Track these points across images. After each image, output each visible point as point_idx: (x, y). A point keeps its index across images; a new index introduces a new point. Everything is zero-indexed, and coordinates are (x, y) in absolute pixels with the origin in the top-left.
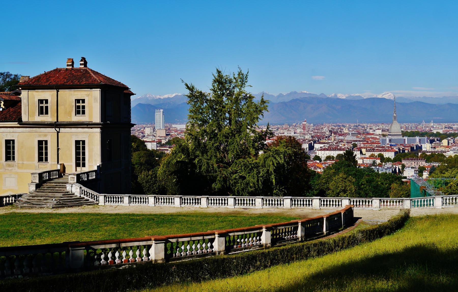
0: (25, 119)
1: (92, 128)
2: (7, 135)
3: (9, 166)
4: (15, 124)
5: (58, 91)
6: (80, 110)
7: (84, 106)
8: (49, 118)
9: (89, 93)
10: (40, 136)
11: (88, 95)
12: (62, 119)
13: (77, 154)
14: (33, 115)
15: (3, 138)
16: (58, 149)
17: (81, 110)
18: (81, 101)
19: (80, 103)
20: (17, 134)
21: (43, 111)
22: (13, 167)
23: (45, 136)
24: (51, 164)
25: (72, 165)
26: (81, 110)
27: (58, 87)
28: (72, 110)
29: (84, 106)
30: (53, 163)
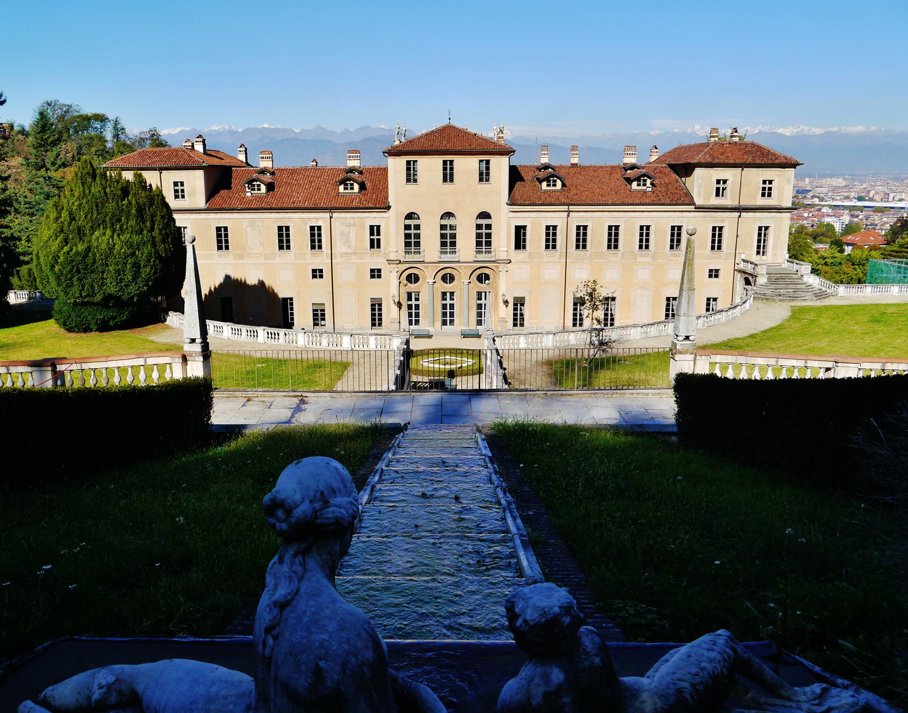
0: (698, 201)
1: (780, 212)
2: (674, 220)
3: (674, 255)
4: (692, 208)
5: (743, 169)
6: (767, 192)
7: (771, 188)
8: (728, 200)
9: (780, 173)
10: (715, 221)
11: (779, 176)
12: (745, 202)
13: (759, 241)
15: (668, 224)
16: (737, 237)
18: (767, 182)
19: (766, 184)
20: (687, 219)
22: (679, 256)
23: (722, 221)
27: (743, 166)
29: (771, 188)
30: (729, 252)
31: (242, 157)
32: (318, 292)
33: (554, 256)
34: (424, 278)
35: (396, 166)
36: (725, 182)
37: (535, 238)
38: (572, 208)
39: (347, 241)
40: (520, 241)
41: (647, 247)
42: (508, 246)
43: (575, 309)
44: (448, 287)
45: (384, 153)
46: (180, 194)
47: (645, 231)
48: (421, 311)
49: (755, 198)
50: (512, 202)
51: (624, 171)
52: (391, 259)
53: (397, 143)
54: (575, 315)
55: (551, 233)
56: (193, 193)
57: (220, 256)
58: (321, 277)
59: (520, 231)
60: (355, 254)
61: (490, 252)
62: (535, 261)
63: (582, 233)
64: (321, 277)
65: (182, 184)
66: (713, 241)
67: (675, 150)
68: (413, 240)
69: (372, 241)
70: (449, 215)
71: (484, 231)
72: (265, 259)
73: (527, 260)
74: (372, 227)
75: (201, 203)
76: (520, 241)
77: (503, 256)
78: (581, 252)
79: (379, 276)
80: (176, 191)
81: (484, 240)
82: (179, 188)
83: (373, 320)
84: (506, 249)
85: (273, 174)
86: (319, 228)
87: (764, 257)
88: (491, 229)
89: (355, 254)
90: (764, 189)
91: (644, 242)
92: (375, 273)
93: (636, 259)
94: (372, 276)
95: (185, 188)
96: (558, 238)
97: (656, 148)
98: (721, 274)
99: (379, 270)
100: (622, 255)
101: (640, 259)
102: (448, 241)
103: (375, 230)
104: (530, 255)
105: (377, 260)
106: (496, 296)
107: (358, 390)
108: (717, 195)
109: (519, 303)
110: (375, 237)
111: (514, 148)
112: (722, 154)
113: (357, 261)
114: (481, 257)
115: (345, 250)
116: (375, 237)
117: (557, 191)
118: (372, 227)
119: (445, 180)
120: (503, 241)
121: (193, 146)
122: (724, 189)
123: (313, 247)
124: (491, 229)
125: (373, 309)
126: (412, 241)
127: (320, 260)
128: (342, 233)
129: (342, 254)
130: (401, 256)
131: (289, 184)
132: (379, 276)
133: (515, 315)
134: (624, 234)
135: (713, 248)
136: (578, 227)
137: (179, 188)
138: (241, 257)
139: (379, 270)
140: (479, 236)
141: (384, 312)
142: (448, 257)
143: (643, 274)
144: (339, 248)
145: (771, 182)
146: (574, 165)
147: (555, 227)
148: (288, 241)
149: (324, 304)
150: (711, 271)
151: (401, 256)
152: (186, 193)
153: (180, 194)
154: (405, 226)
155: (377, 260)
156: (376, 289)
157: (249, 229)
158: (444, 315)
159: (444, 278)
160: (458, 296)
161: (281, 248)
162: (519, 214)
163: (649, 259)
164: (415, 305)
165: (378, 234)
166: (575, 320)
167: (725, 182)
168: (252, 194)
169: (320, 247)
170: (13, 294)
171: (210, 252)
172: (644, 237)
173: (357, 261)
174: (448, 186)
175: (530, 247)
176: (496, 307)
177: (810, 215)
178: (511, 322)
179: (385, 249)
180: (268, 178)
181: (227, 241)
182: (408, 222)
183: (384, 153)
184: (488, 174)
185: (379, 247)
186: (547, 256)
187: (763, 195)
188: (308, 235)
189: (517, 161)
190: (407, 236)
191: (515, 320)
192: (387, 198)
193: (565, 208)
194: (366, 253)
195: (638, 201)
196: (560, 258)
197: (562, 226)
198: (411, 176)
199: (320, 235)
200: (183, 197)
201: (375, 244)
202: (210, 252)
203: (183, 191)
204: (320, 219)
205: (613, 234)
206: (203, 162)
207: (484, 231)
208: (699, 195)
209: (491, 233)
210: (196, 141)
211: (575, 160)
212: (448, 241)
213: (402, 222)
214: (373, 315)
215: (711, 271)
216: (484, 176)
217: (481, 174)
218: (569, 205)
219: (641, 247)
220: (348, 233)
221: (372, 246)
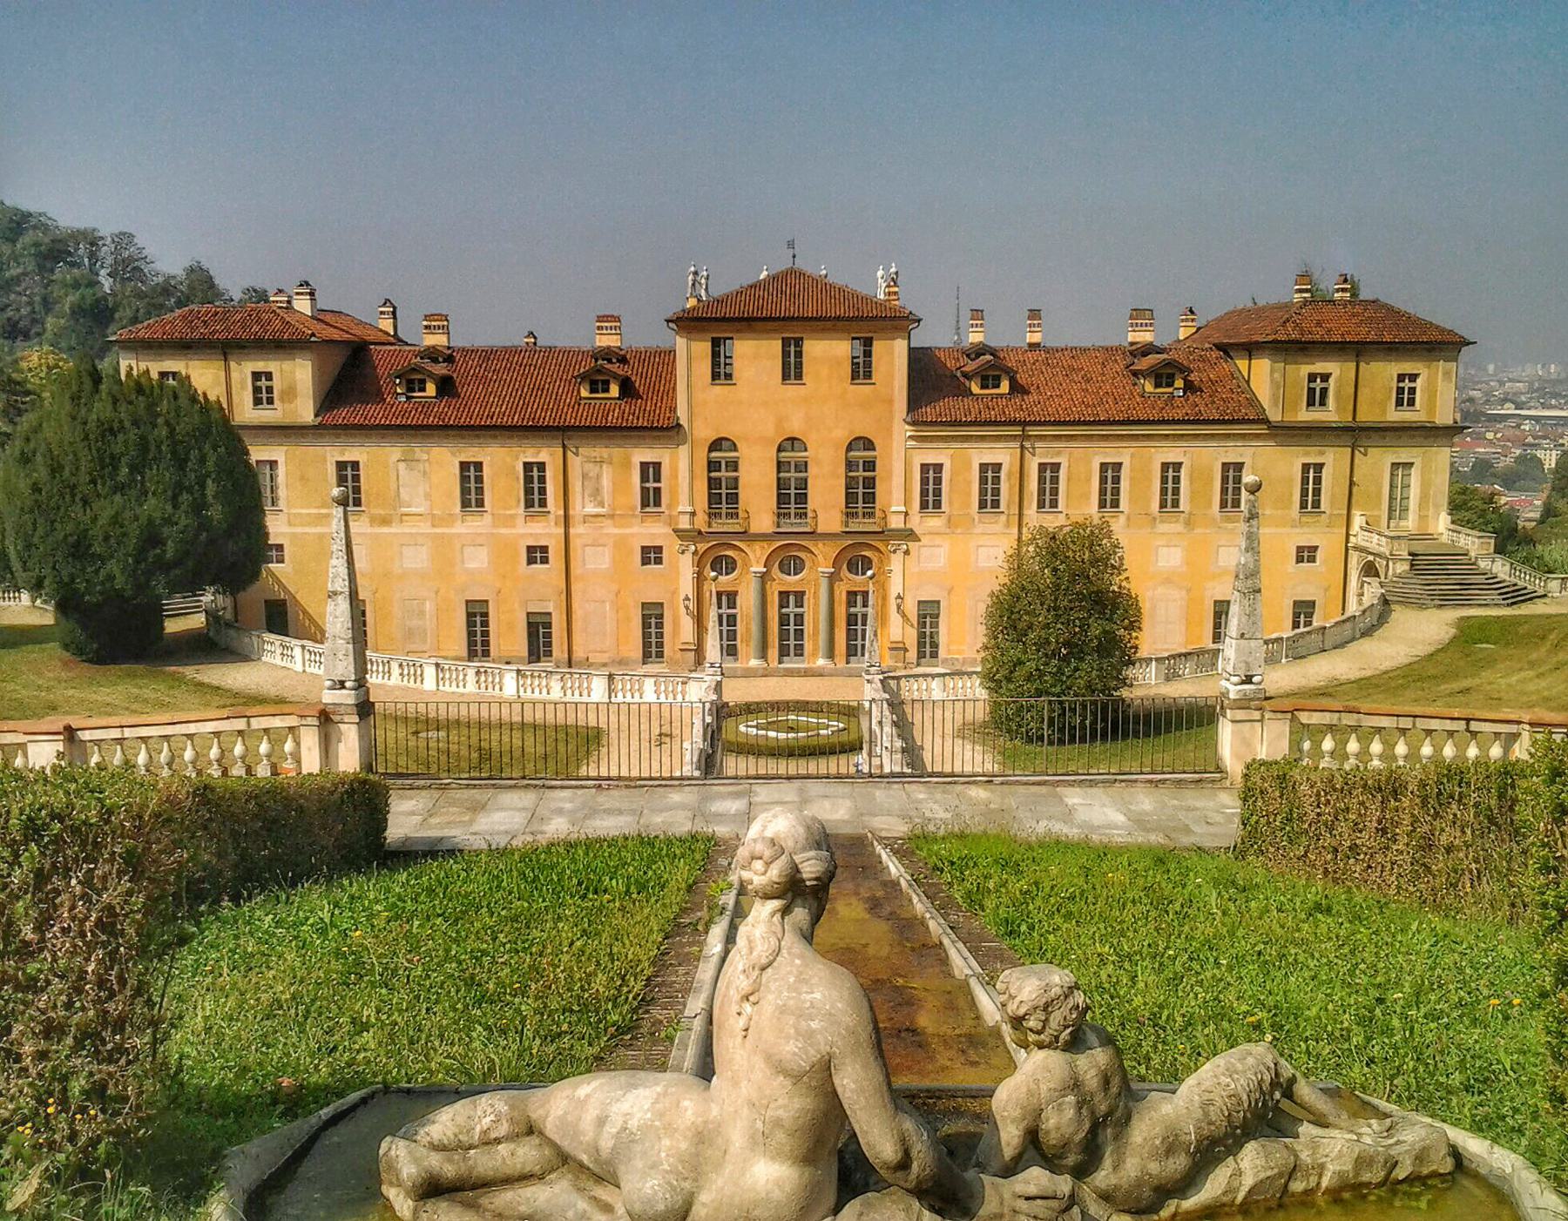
3: (1229, 520)
6: (1405, 398)
8: (1330, 414)
14: (1295, 409)
16: (1352, 483)
17: (1406, 396)
21: (1316, 398)
24: (1331, 515)
25: (1379, 517)
26: (1406, 396)
28: (1390, 397)
31: (386, 325)
33: (996, 522)
34: (747, 565)
35: (692, 354)
36: (1325, 377)
37: (961, 487)
39: (597, 492)
40: (931, 498)
45: (668, 321)
46: (264, 395)
48: (740, 628)
49: (1383, 405)
51: (1129, 359)
52: (681, 526)
53: (692, 302)
56: (290, 393)
58: (545, 560)
59: (931, 475)
60: (612, 516)
61: (872, 515)
62: (959, 531)
64: (545, 560)
65: (269, 376)
66: (1304, 493)
67: (1229, 314)
68: (724, 491)
69: (645, 491)
72: (433, 526)
73: (943, 530)
75: (305, 411)
76: (931, 495)
77: (896, 522)
79: (659, 561)
80: (257, 390)
82: (263, 383)
84: (903, 509)
85: (449, 359)
87: (1403, 523)
88: (874, 470)
90: (1400, 391)
91: (1169, 498)
92: (651, 555)
93: (1153, 526)
94: (645, 561)
95: (276, 384)
96: (1004, 487)
97: (1192, 312)
98: (1319, 555)
99: (659, 549)
100: (1128, 519)
101: (1163, 528)
103: (650, 471)
104: (949, 521)
105: (655, 531)
106: (885, 598)
107: (647, 775)
108: (1311, 403)
110: (651, 485)
111: (919, 313)
112: (1319, 324)
113: (616, 531)
114: (854, 526)
115: (591, 509)
116: (651, 485)
117: (1001, 396)
119: (785, 376)
120: (898, 494)
121: (289, 302)
122: (1324, 391)
123: (529, 504)
124: (874, 470)
127: (545, 531)
128: (585, 476)
129: (586, 518)
130: (701, 522)
131: (485, 381)
132: (659, 561)
133: (922, 635)
134: (1131, 479)
135: (1303, 505)
136: (1042, 467)
137: (263, 383)
138: (385, 521)
139: (659, 549)
141: (667, 629)
144: (583, 506)
145: (1413, 377)
146: (1034, 346)
147: (997, 467)
148: (480, 491)
149: (550, 614)
151: (701, 522)
152: (276, 395)
153: (264, 395)
154: (709, 462)
155: (655, 531)
156: (650, 585)
157: (402, 466)
160: (812, 601)
163: (1179, 527)
164: (728, 616)
165: (658, 479)
168: (408, 398)
169: (543, 503)
170: (433, 668)
171: (324, 511)
172: (1170, 485)
173: (616, 531)
174: (792, 390)
175: (951, 503)
177: (1499, 435)
179: (669, 507)
180: (441, 369)
183: (668, 321)
184: (868, 365)
185: (658, 503)
186: (980, 522)
187: (1399, 403)
188: (518, 478)
189: (921, 338)
190: (713, 483)
191: (921, 645)
192: (673, 410)
193: (1017, 431)
194: (633, 516)
196: (1008, 525)
197: (1011, 464)
198: (721, 372)
199: (542, 480)
200: (270, 401)
201: (651, 498)
202: (324, 511)
203: (270, 390)
206: (313, 335)
208: (1276, 404)
209: (874, 478)
210: (298, 294)
211: (1036, 338)
213: (702, 455)
215: (1300, 549)
216: (861, 370)
217: (855, 365)
218: (1024, 424)
219: (1163, 505)
220: (598, 477)
221: (645, 504)
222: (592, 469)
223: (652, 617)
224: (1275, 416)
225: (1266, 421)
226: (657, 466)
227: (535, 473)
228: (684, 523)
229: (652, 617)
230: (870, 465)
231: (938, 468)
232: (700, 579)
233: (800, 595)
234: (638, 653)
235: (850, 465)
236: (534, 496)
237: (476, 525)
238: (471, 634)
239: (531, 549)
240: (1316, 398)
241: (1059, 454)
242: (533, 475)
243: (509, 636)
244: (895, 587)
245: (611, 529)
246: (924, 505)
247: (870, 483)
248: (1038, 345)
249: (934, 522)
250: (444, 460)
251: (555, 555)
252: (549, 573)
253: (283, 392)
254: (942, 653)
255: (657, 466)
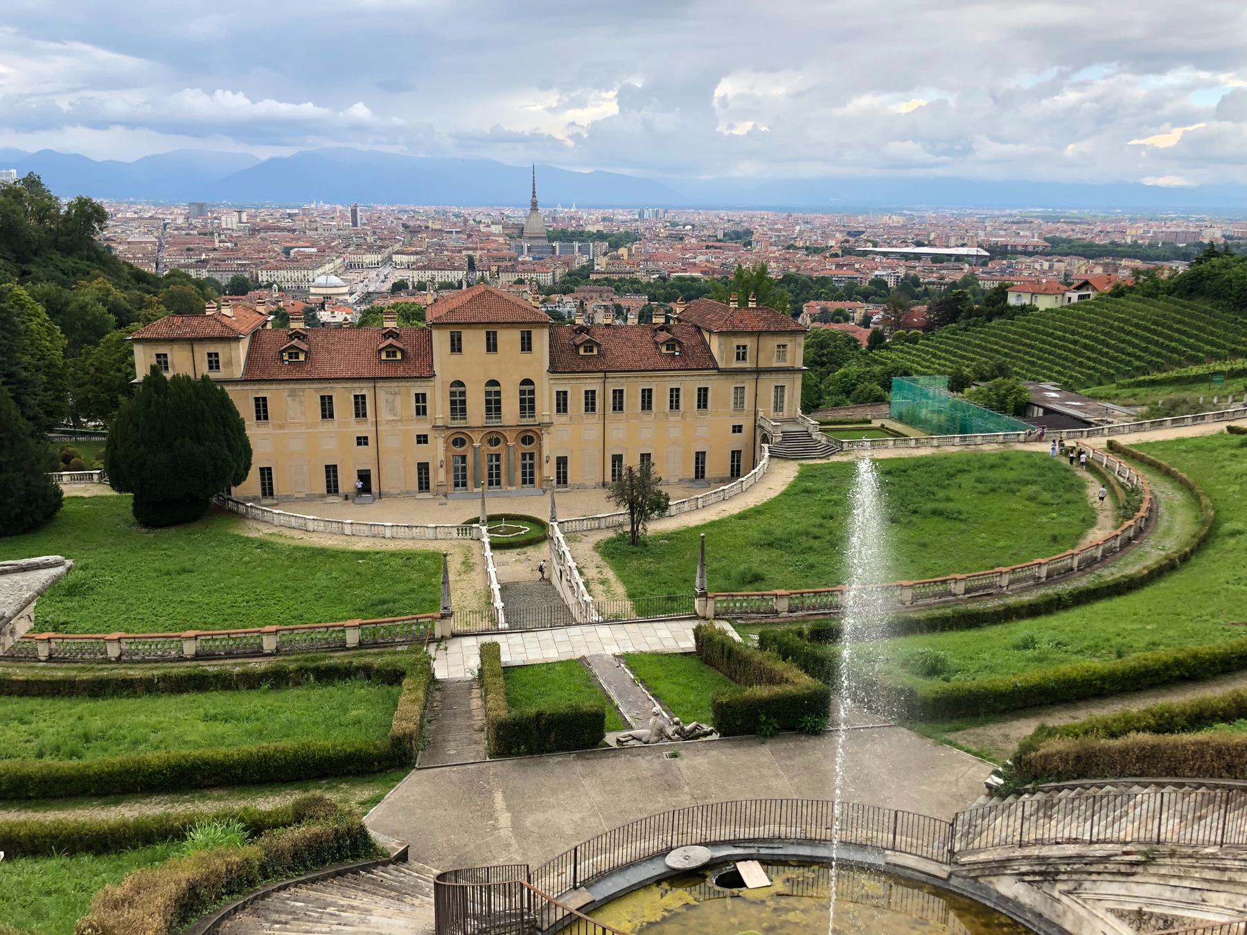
3: (702, 414)
8: (747, 365)
12: (762, 365)
21: (741, 356)
32: (364, 458)
36: (744, 347)
37: (576, 402)
38: (608, 375)
41: (677, 407)
42: (550, 411)
43: (614, 466)
44: (494, 449)
46: (214, 365)
47: (675, 393)
49: (771, 359)
50: (553, 370)
54: (614, 471)
55: (590, 397)
56: (229, 363)
57: (258, 427)
58: (366, 444)
60: (401, 421)
63: (618, 394)
64: (366, 444)
65: (217, 355)
69: (418, 408)
70: (493, 383)
71: (527, 396)
74: (417, 395)
77: (547, 420)
78: (618, 415)
79: (426, 442)
80: (210, 362)
81: (527, 404)
82: (214, 358)
83: (420, 483)
86: (363, 397)
89: (401, 421)
91: (675, 403)
92: (422, 439)
94: (419, 442)
98: (744, 429)
99: (426, 436)
101: (671, 419)
102: (493, 406)
103: (421, 398)
105: (423, 427)
108: (738, 358)
109: (562, 462)
110: (421, 404)
112: (741, 322)
118: (417, 395)
119: (488, 350)
120: (546, 405)
122: (744, 353)
123: (357, 415)
125: (420, 474)
126: (458, 406)
128: (387, 401)
129: (388, 422)
132: (426, 442)
133: (558, 473)
136: (614, 391)
138: (282, 427)
139: (426, 436)
140: (522, 401)
142: (494, 422)
143: (674, 433)
144: (385, 415)
147: (593, 392)
150: (734, 427)
153: (214, 365)
154: (451, 393)
157: (289, 399)
158: (490, 475)
159: (490, 441)
161: (324, 416)
162: (560, 382)
163: (679, 418)
165: (424, 401)
166: (613, 475)
167: (744, 347)
169: (365, 415)
176: (540, 467)
178: (555, 482)
181: (266, 411)
182: (454, 389)
185: (425, 413)
190: (453, 403)
191: (558, 477)
192: (431, 366)
193: (602, 375)
195: (668, 367)
196: (599, 419)
198: (456, 346)
199: (364, 403)
200: (218, 367)
201: (421, 411)
203: (217, 362)
204: (365, 389)
205: (647, 396)
207: (527, 396)
212: (493, 406)
213: (448, 389)
214: (420, 479)
215: (734, 427)
216: (526, 345)
218: (605, 372)
219: (671, 407)
220: (393, 401)
221: (418, 413)
222: (391, 398)
223: (423, 468)
224: (721, 365)
225: (717, 368)
226: (424, 395)
227: (360, 400)
228: (439, 423)
229: (423, 468)
230: (532, 392)
231: (565, 393)
232: (447, 450)
233: (498, 457)
234: (417, 488)
235: (522, 392)
236: (360, 411)
237: (328, 426)
238: (328, 482)
239: (358, 438)
240: (741, 356)
241: (622, 385)
242: (360, 401)
243: (349, 481)
244: (545, 453)
245: (400, 426)
246: (558, 411)
247: (532, 401)
248: (609, 325)
249: (563, 418)
250: (311, 396)
251: (371, 441)
252: (368, 450)
253: (224, 363)
254: (569, 481)
255: (424, 395)
